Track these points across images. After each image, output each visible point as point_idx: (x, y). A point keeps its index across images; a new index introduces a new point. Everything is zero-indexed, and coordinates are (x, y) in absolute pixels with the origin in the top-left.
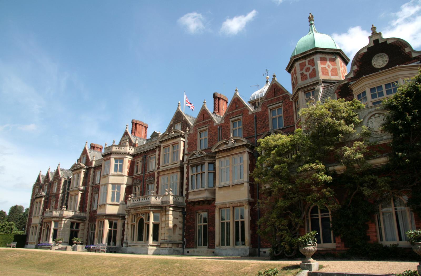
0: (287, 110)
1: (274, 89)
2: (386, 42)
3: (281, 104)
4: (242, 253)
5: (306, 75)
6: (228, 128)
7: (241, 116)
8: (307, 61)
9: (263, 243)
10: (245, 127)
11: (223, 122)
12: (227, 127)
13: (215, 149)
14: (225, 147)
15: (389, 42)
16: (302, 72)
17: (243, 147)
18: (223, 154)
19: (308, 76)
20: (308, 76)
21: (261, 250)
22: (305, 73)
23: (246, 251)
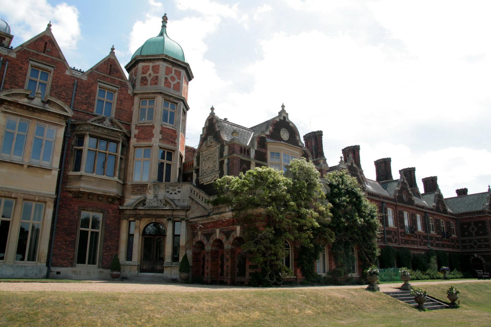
0: (121, 101)
1: (111, 66)
2: (289, 123)
3: (117, 89)
4: (33, 273)
5: (170, 83)
6: (22, 72)
7: (52, 69)
8: (174, 69)
9: (56, 259)
10: (54, 87)
11: (67, 73)
12: (21, 68)
13: (6, 95)
14: (24, 101)
15: (291, 124)
16: (167, 76)
17: (61, 118)
18: (17, 109)
19: (172, 86)
20: (172, 86)
21: (52, 269)
22: (169, 79)
23: (41, 271)
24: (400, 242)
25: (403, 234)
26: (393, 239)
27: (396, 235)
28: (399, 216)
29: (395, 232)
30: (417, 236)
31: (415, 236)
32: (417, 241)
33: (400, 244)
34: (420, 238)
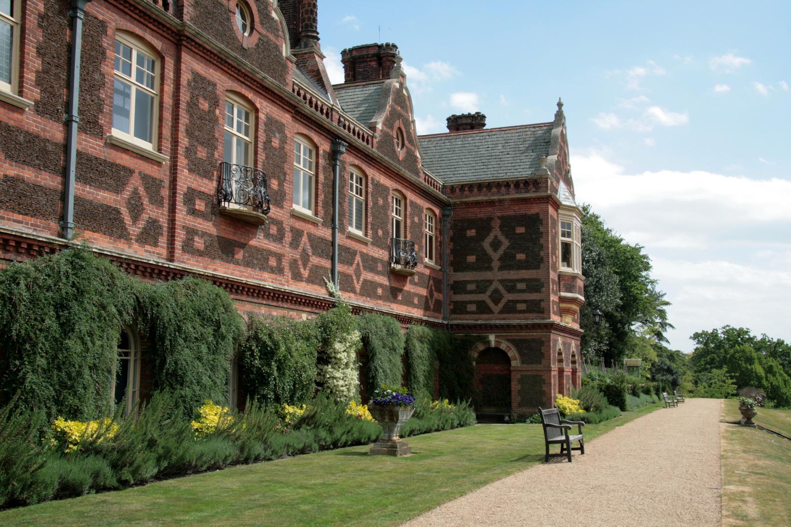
24: (178, 244)
25: (200, 205)
26: (128, 220)
27: (157, 201)
28: (192, 105)
29: (152, 185)
30: (281, 231)
31: (274, 230)
32: (279, 257)
33: (178, 252)
34: (295, 244)
